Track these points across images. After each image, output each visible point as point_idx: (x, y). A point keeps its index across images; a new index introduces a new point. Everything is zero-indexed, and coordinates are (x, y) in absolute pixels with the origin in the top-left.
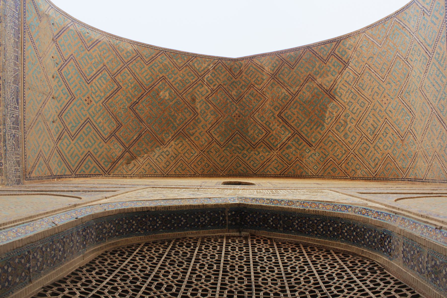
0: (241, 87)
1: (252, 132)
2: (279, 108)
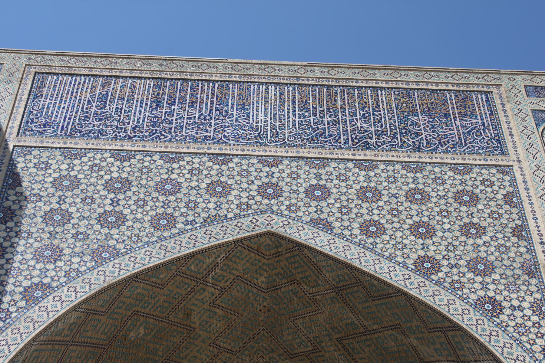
0: (276, 275)
1: (290, 338)
2: (340, 332)
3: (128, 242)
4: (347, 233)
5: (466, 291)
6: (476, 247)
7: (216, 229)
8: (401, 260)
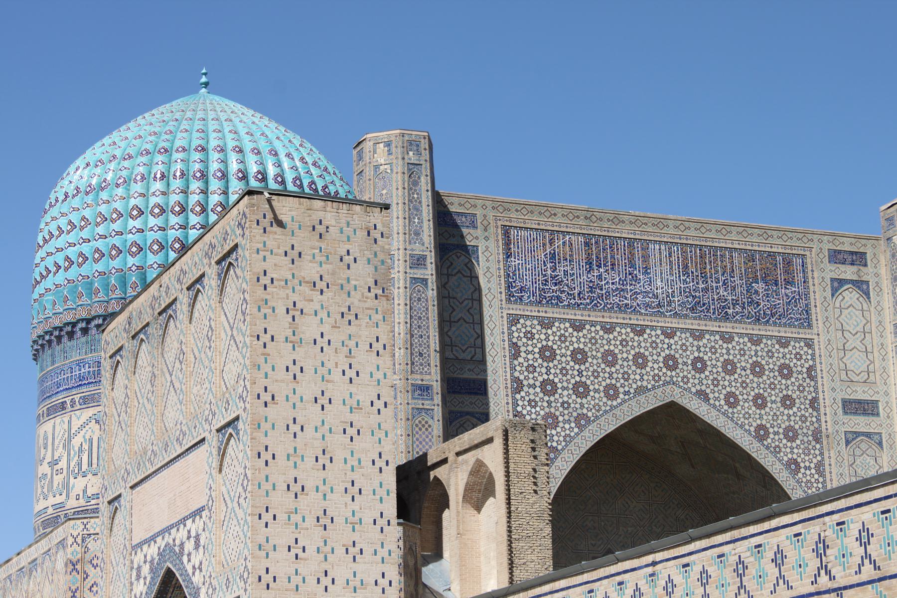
3: (593, 411)
4: (717, 403)
5: (782, 454)
6: (789, 416)
7: (642, 398)
8: (747, 427)
